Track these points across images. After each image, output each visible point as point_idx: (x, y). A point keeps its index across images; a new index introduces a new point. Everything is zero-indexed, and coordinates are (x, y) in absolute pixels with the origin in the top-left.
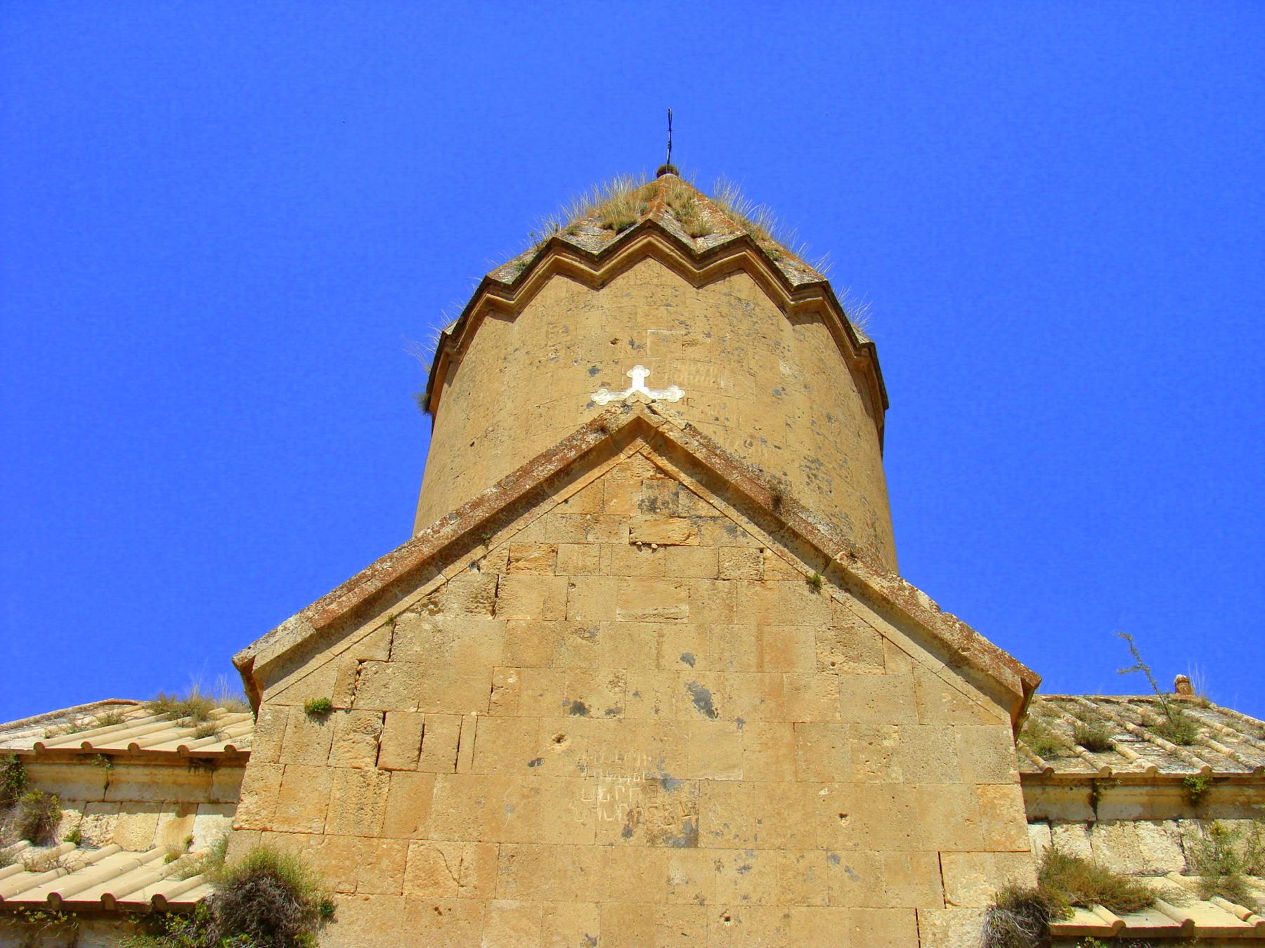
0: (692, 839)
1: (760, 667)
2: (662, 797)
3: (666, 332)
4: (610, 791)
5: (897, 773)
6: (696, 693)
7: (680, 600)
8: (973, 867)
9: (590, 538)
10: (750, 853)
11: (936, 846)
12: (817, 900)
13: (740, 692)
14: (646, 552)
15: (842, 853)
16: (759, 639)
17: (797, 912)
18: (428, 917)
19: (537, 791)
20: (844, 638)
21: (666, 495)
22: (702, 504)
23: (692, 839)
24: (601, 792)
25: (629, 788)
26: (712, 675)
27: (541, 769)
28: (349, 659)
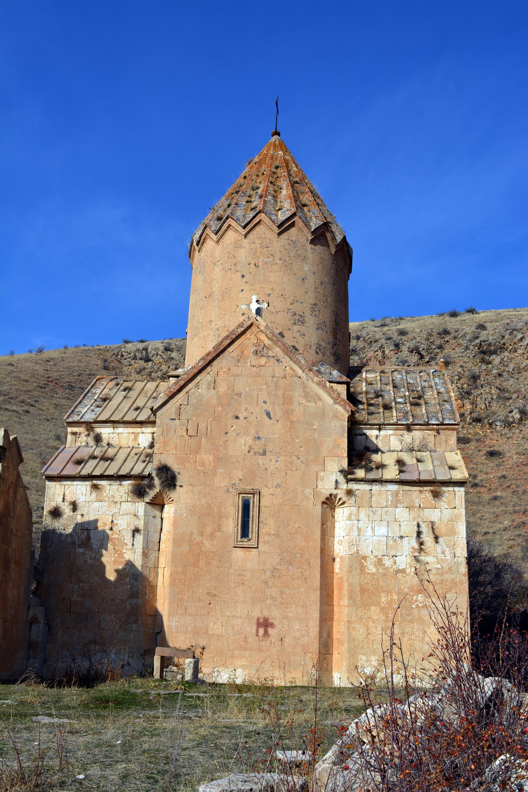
0: (264, 453)
1: (283, 404)
2: (258, 442)
3: (266, 260)
4: (245, 441)
5: (316, 435)
6: (267, 413)
7: (263, 384)
8: (332, 461)
9: (239, 364)
10: (278, 457)
11: (324, 455)
12: (293, 469)
13: (278, 412)
14: (254, 369)
15: (301, 457)
16: (283, 396)
17: (289, 472)
18: (202, 475)
19: (227, 441)
20: (307, 395)
21: (260, 349)
22: (270, 352)
23: (264, 453)
24: (243, 441)
25: (249, 440)
26: (271, 407)
27: (228, 435)
28: (178, 404)
